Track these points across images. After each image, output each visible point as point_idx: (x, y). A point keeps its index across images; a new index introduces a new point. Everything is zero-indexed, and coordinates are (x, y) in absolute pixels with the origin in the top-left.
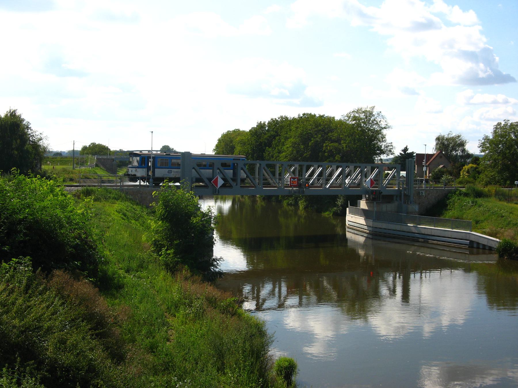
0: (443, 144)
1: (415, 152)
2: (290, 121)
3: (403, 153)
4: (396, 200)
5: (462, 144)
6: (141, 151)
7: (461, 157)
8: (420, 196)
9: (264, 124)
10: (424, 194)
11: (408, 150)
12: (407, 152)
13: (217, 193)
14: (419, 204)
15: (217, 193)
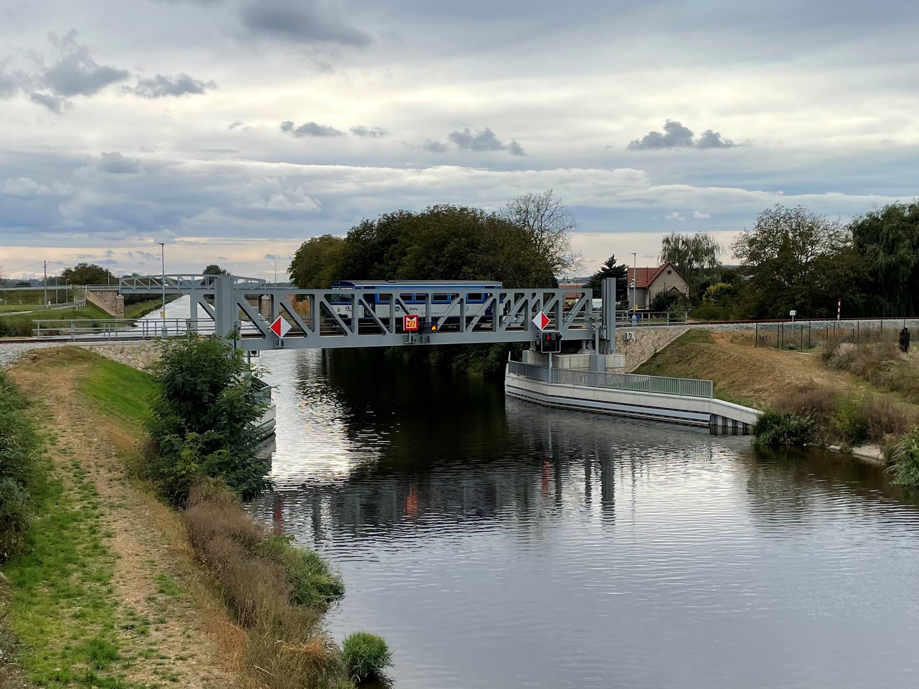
0: (676, 250)
1: (627, 265)
2: (414, 219)
3: (608, 268)
4: (587, 348)
5: (710, 251)
6: (179, 276)
7: (708, 272)
8: (628, 340)
9: (371, 225)
10: (633, 337)
11: (615, 262)
12: (614, 266)
13: (280, 346)
14: (626, 354)
15: (280, 346)
